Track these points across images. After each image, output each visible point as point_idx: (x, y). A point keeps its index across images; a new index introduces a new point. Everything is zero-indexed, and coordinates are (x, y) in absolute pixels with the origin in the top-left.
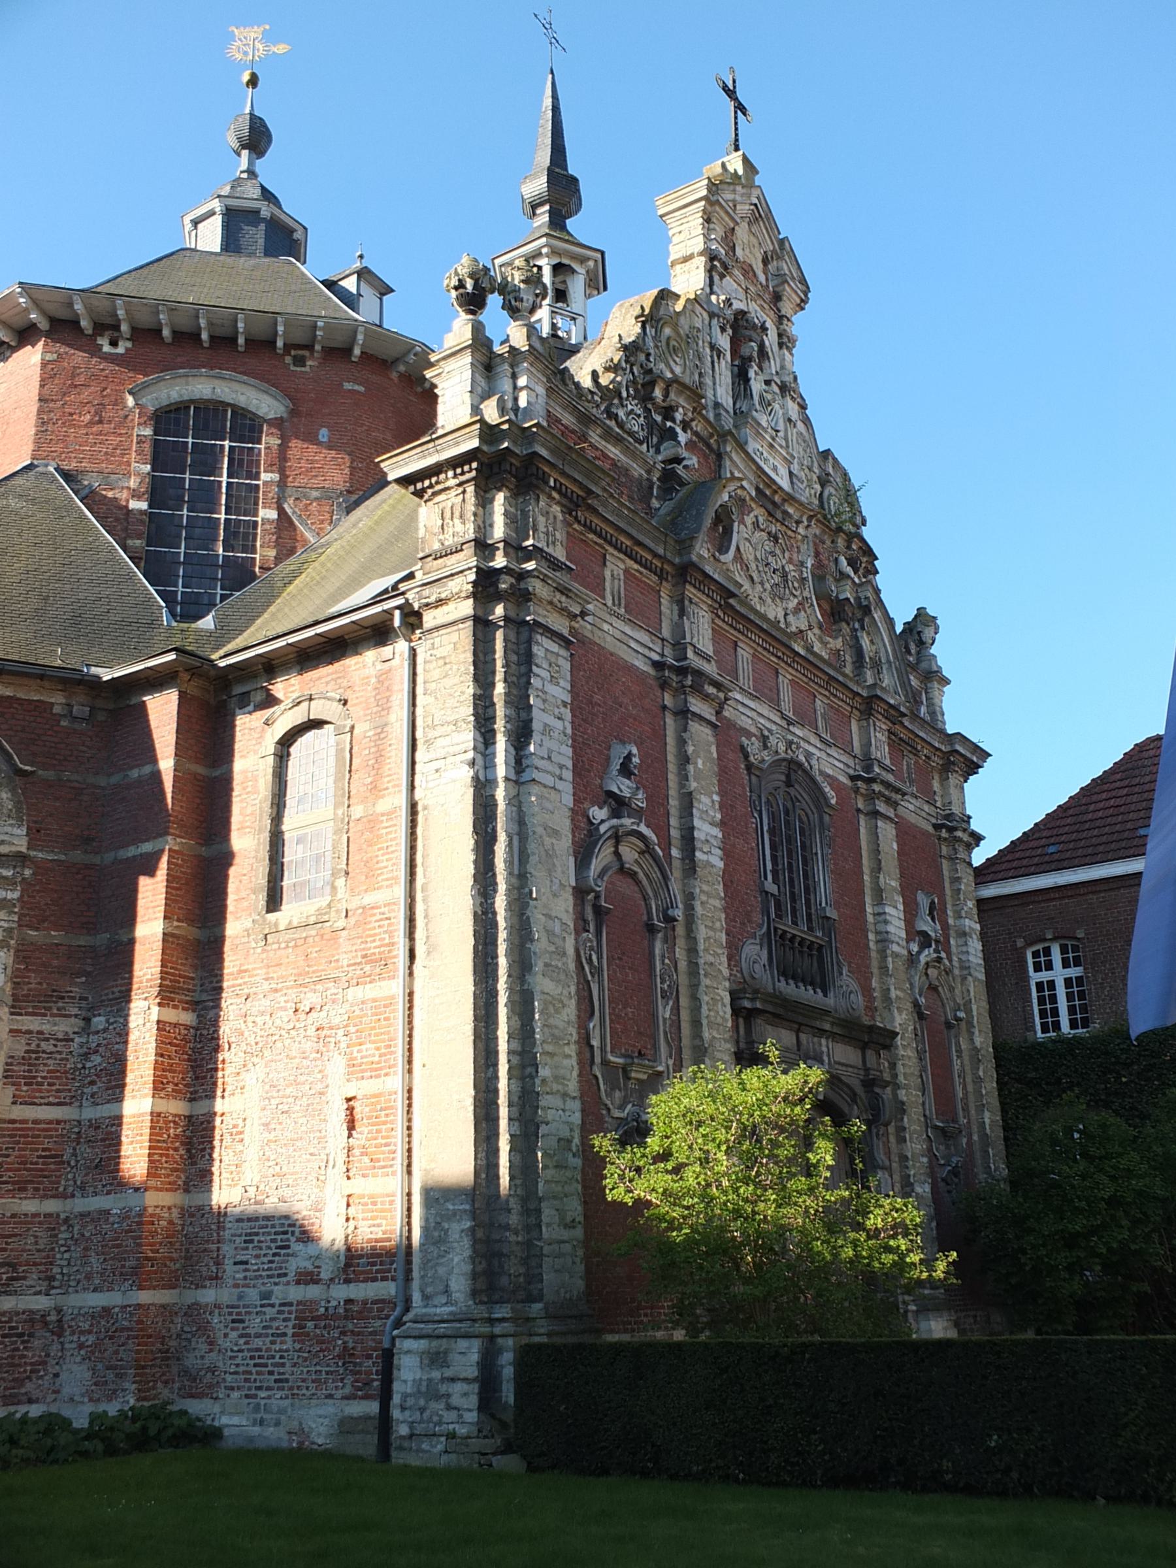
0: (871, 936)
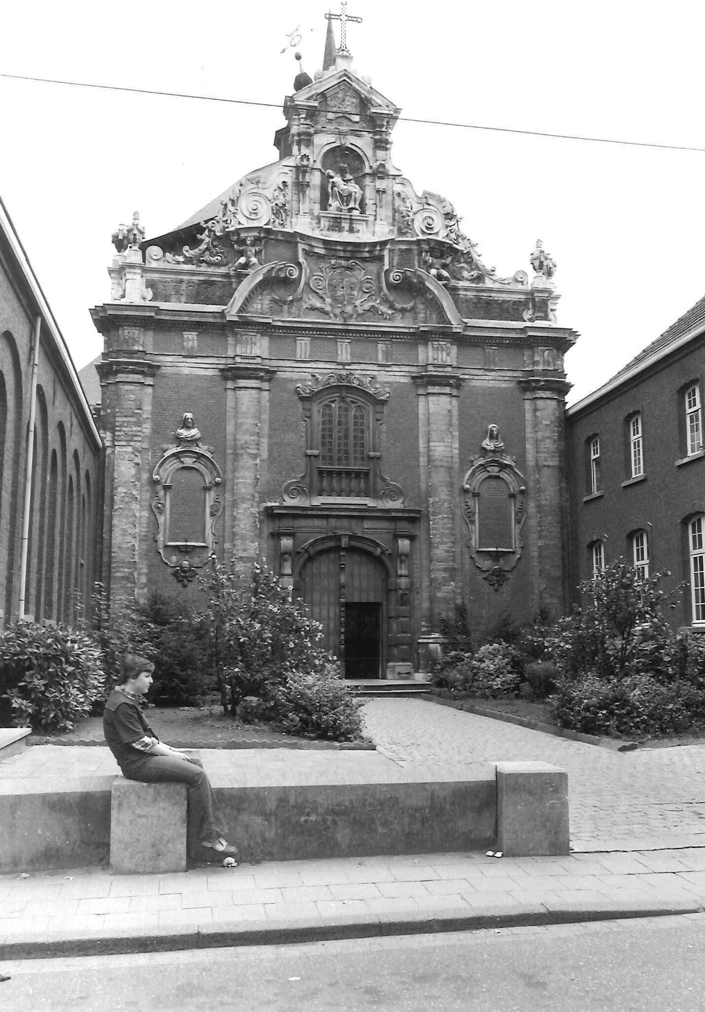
0: (421, 459)
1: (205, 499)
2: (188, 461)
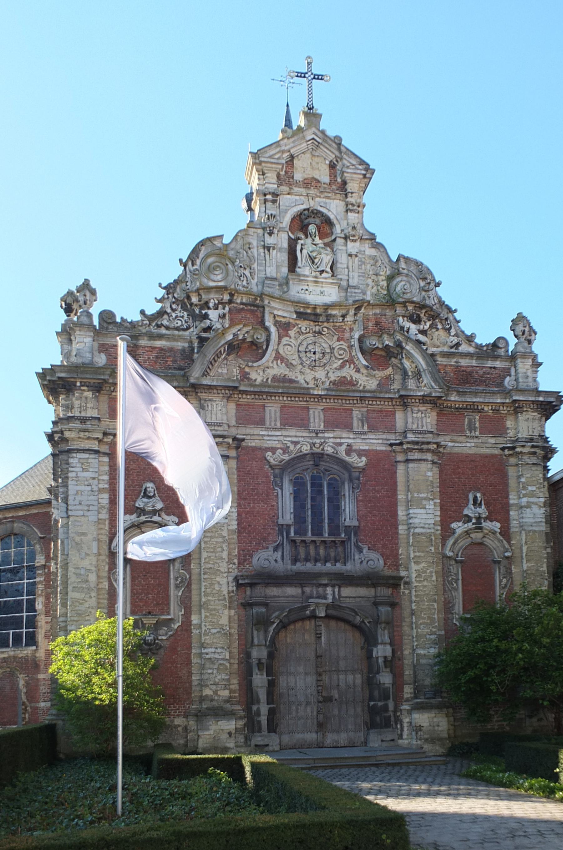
0: (400, 527)
1: (169, 571)
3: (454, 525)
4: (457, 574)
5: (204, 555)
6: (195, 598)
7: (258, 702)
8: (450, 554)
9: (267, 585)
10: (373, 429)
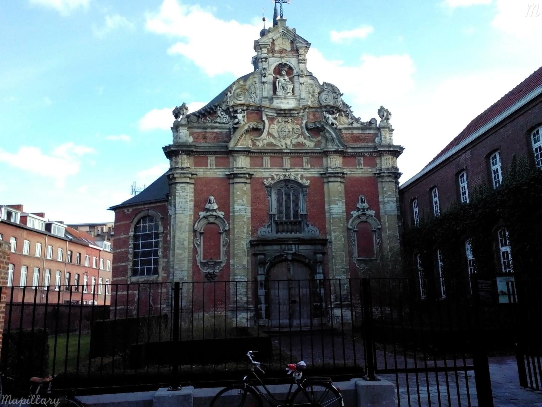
0: (326, 214)
2: (212, 220)
3: (352, 213)
4: (354, 237)
5: (236, 230)
6: (231, 251)
7: (261, 303)
8: (350, 227)
9: (264, 245)
10: (313, 166)
